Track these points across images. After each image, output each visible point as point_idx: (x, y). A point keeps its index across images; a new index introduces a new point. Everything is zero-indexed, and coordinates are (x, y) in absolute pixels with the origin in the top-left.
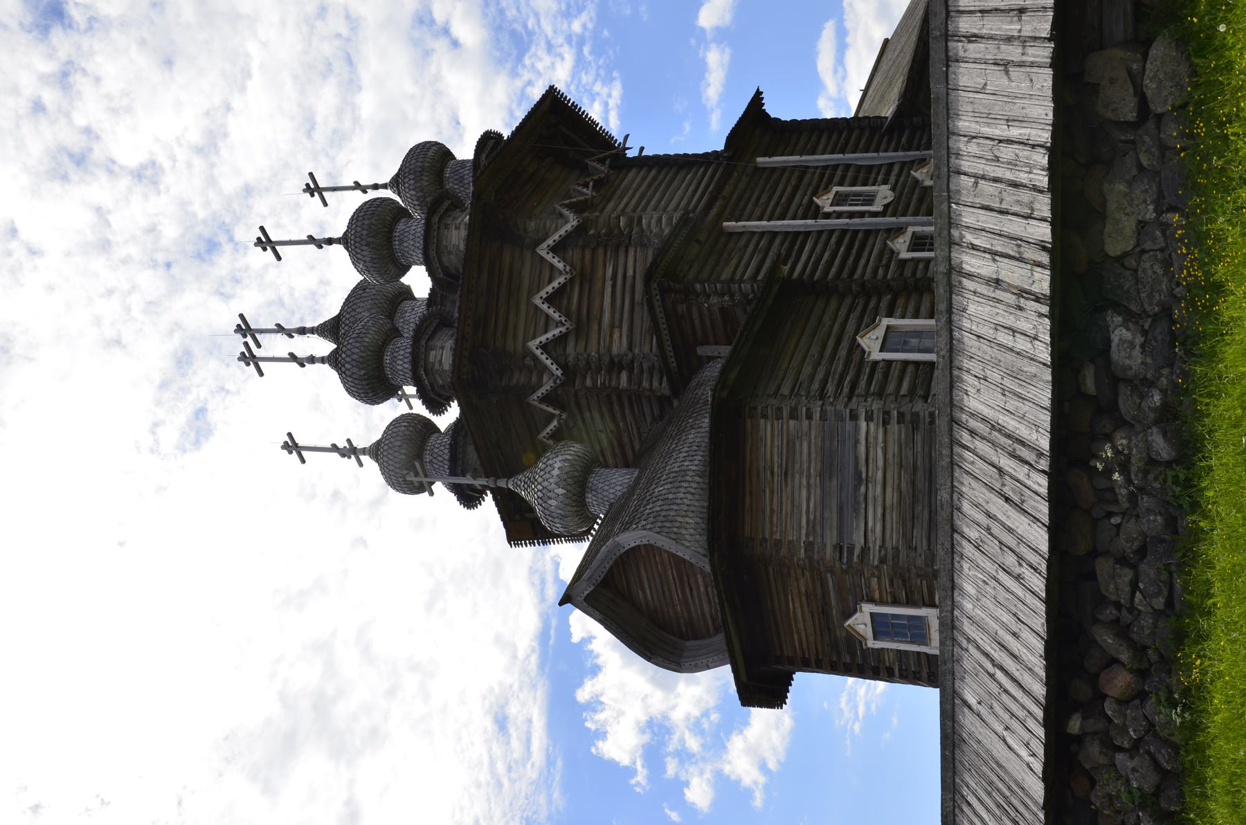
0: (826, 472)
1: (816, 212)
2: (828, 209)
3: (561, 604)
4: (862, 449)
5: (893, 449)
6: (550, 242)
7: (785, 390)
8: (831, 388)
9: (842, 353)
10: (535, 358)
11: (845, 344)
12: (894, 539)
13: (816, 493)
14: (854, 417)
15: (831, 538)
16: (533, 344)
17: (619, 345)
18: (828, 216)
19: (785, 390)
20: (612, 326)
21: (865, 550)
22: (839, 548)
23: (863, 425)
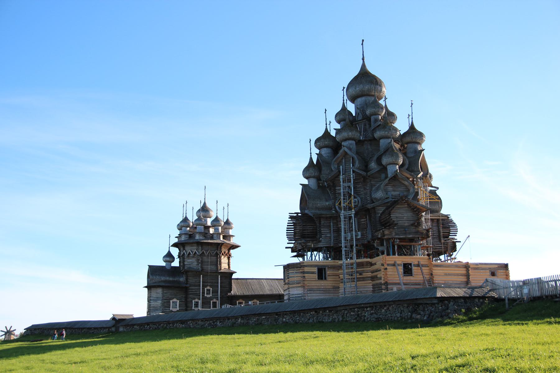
0: (157, 298)
1: (204, 286)
2: (206, 289)
3: (148, 265)
4: (158, 301)
5: (159, 305)
6: (196, 251)
7: (165, 292)
8: (166, 297)
9: (172, 297)
10: (183, 251)
11: (174, 297)
12: (152, 306)
13: (155, 297)
14: (161, 300)
15: (152, 299)
16: (184, 251)
17: (186, 263)
18: (203, 289)
19: (165, 292)
20: (188, 262)
21: (150, 303)
22: (151, 299)
23: (160, 301)
